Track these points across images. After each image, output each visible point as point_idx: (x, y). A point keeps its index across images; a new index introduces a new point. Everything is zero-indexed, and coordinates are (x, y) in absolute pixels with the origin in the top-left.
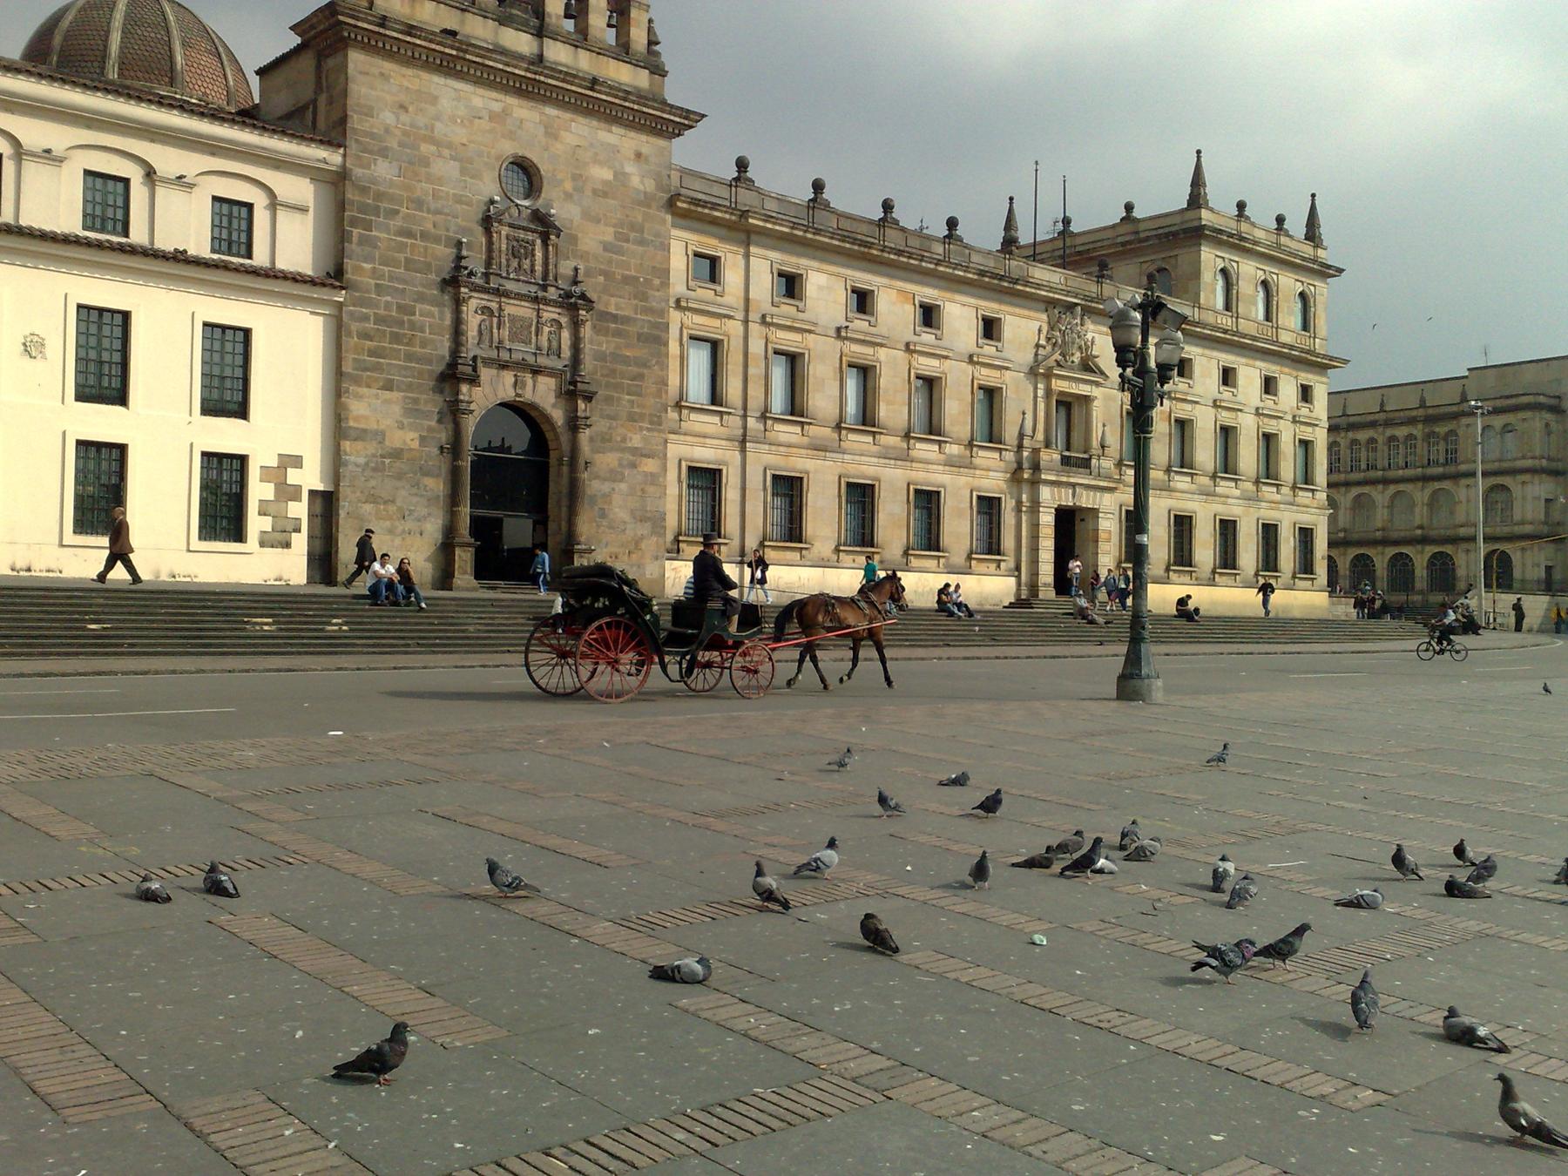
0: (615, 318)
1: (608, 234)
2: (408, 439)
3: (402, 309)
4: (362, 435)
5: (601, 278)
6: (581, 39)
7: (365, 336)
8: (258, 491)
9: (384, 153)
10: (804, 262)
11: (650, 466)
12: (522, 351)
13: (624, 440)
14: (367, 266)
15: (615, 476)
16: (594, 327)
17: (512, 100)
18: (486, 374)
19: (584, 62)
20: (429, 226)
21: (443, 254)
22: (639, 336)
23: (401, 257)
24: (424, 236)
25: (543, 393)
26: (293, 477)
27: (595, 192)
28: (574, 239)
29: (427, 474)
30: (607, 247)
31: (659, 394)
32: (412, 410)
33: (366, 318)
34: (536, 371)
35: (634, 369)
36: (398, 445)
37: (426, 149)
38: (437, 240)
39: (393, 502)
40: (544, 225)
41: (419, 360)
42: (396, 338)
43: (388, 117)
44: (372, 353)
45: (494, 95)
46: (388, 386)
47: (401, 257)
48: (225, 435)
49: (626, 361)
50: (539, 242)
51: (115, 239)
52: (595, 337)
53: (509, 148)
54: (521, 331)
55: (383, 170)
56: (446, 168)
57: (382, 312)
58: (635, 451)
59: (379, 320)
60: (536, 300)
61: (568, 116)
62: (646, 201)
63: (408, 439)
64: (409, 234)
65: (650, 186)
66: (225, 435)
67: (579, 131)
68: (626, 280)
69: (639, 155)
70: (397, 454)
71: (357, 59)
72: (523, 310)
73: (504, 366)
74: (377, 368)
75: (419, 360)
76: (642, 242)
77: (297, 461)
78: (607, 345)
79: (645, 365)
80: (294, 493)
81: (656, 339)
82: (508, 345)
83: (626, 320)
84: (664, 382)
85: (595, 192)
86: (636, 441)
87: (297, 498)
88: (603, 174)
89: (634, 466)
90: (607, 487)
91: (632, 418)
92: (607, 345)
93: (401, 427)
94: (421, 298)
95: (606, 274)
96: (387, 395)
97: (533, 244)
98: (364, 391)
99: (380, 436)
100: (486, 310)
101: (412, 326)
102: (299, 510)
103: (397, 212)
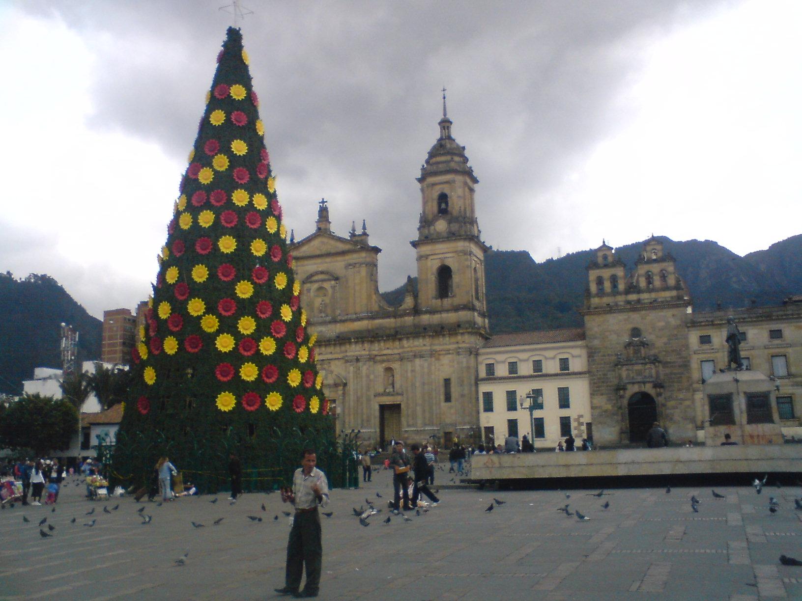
0: (670, 362)
1: (665, 340)
2: (609, 407)
3: (604, 375)
4: (596, 408)
5: (664, 353)
6: (650, 291)
7: (596, 383)
8: (573, 424)
9: (595, 338)
10: (746, 328)
11: (688, 403)
12: (639, 379)
13: (676, 397)
14: (594, 366)
15: (675, 408)
16: (663, 367)
17: (631, 314)
18: (629, 386)
19: (653, 295)
20: (610, 353)
21: (614, 358)
22: (679, 366)
23: (602, 362)
24: (608, 355)
25: (649, 389)
26: (582, 420)
27: (659, 330)
28: (653, 344)
29: (614, 414)
30: (665, 344)
31: (688, 381)
32: (609, 400)
33: (594, 379)
34: (644, 383)
35: (678, 376)
36: (606, 409)
37: (607, 334)
38: (612, 355)
39: (606, 423)
40: (643, 344)
41: (610, 386)
42: (603, 382)
43: (596, 329)
44: (597, 387)
45: (625, 314)
46: (602, 394)
47: (602, 362)
48: (565, 413)
49: (675, 374)
50: (642, 348)
51: (539, 373)
52: (663, 369)
53: (630, 326)
54: (639, 373)
55: (596, 342)
56: (614, 337)
57: (599, 376)
58: (682, 399)
59: (599, 379)
60: (642, 364)
61: (648, 312)
62: (677, 327)
63: (609, 407)
64: (604, 356)
65: (678, 322)
66: (565, 413)
67: (652, 316)
68: (673, 351)
69: (673, 315)
70: (606, 411)
71: (586, 318)
72: (639, 367)
73: (633, 383)
74: (599, 390)
75: (610, 386)
76: (676, 339)
77: (582, 416)
78: (668, 371)
79: (682, 373)
80: (582, 424)
81: (686, 365)
82: (635, 377)
83: (674, 362)
84: (689, 378)
85: (659, 330)
86: (681, 396)
87: (582, 424)
88: (662, 324)
89: (681, 404)
90: (672, 411)
91: (679, 390)
92: (668, 371)
93: (606, 404)
94: (609, 371)
95: (665, 351)
96: (601, 397)
97: (641, 349)
98: (596, 397)
99: (600, 407)
100: (627, 370)
101: (607, 378)
102: (584, 428)
103: (600, 352)
